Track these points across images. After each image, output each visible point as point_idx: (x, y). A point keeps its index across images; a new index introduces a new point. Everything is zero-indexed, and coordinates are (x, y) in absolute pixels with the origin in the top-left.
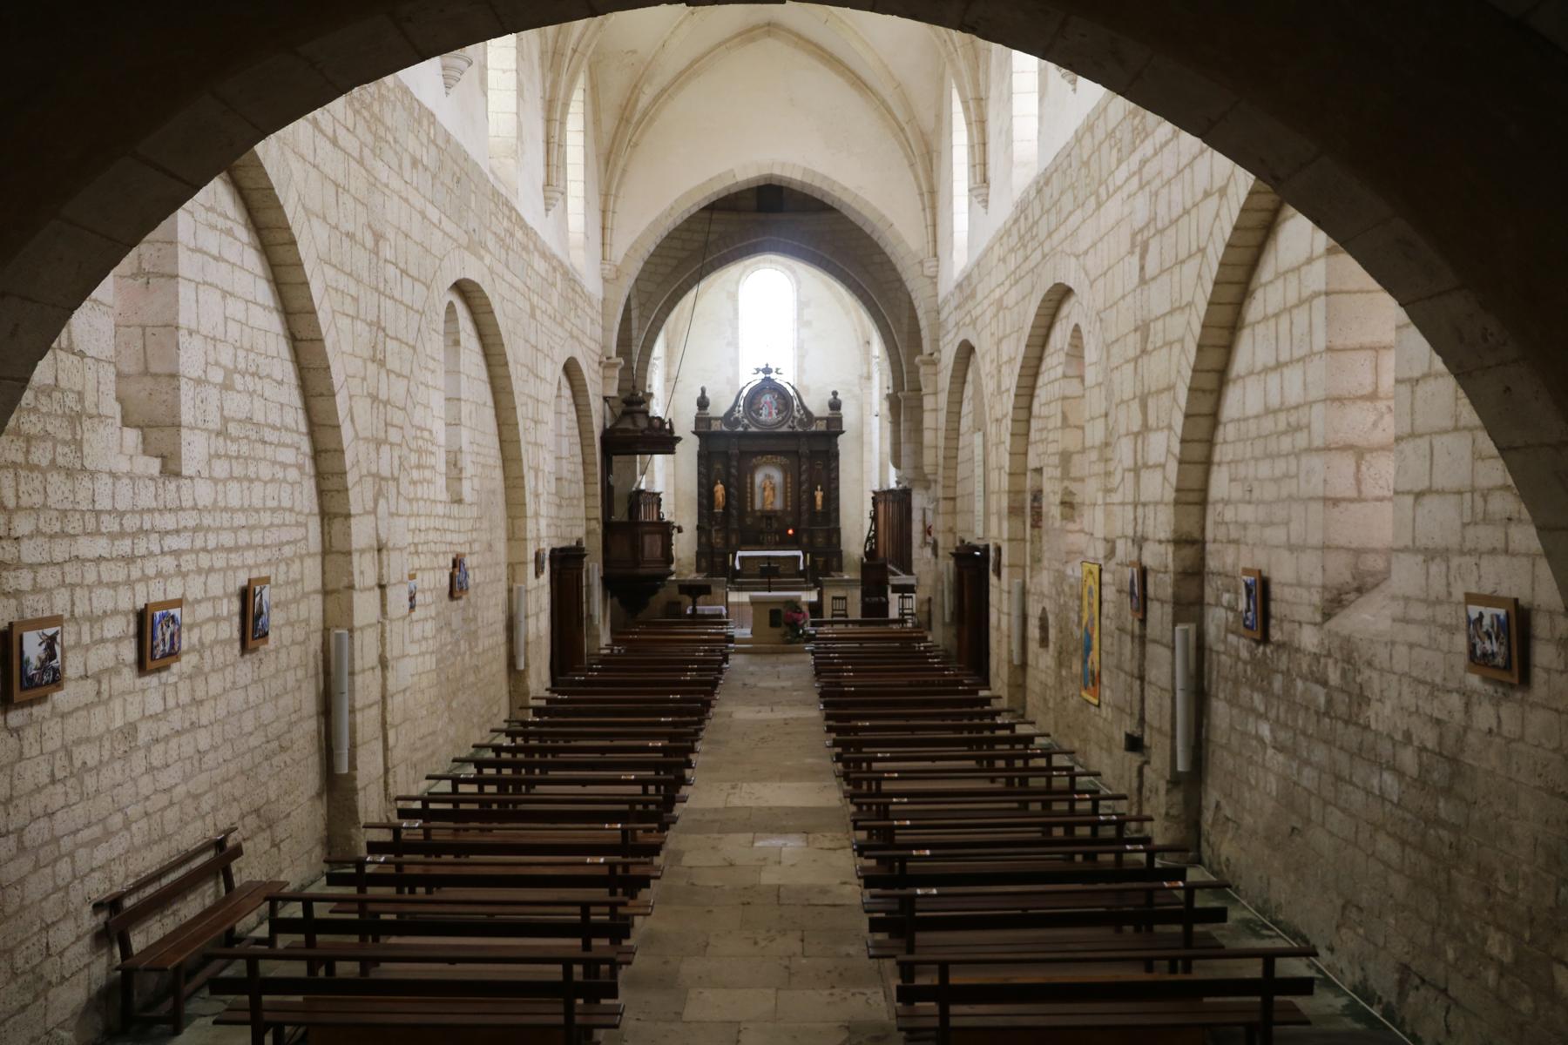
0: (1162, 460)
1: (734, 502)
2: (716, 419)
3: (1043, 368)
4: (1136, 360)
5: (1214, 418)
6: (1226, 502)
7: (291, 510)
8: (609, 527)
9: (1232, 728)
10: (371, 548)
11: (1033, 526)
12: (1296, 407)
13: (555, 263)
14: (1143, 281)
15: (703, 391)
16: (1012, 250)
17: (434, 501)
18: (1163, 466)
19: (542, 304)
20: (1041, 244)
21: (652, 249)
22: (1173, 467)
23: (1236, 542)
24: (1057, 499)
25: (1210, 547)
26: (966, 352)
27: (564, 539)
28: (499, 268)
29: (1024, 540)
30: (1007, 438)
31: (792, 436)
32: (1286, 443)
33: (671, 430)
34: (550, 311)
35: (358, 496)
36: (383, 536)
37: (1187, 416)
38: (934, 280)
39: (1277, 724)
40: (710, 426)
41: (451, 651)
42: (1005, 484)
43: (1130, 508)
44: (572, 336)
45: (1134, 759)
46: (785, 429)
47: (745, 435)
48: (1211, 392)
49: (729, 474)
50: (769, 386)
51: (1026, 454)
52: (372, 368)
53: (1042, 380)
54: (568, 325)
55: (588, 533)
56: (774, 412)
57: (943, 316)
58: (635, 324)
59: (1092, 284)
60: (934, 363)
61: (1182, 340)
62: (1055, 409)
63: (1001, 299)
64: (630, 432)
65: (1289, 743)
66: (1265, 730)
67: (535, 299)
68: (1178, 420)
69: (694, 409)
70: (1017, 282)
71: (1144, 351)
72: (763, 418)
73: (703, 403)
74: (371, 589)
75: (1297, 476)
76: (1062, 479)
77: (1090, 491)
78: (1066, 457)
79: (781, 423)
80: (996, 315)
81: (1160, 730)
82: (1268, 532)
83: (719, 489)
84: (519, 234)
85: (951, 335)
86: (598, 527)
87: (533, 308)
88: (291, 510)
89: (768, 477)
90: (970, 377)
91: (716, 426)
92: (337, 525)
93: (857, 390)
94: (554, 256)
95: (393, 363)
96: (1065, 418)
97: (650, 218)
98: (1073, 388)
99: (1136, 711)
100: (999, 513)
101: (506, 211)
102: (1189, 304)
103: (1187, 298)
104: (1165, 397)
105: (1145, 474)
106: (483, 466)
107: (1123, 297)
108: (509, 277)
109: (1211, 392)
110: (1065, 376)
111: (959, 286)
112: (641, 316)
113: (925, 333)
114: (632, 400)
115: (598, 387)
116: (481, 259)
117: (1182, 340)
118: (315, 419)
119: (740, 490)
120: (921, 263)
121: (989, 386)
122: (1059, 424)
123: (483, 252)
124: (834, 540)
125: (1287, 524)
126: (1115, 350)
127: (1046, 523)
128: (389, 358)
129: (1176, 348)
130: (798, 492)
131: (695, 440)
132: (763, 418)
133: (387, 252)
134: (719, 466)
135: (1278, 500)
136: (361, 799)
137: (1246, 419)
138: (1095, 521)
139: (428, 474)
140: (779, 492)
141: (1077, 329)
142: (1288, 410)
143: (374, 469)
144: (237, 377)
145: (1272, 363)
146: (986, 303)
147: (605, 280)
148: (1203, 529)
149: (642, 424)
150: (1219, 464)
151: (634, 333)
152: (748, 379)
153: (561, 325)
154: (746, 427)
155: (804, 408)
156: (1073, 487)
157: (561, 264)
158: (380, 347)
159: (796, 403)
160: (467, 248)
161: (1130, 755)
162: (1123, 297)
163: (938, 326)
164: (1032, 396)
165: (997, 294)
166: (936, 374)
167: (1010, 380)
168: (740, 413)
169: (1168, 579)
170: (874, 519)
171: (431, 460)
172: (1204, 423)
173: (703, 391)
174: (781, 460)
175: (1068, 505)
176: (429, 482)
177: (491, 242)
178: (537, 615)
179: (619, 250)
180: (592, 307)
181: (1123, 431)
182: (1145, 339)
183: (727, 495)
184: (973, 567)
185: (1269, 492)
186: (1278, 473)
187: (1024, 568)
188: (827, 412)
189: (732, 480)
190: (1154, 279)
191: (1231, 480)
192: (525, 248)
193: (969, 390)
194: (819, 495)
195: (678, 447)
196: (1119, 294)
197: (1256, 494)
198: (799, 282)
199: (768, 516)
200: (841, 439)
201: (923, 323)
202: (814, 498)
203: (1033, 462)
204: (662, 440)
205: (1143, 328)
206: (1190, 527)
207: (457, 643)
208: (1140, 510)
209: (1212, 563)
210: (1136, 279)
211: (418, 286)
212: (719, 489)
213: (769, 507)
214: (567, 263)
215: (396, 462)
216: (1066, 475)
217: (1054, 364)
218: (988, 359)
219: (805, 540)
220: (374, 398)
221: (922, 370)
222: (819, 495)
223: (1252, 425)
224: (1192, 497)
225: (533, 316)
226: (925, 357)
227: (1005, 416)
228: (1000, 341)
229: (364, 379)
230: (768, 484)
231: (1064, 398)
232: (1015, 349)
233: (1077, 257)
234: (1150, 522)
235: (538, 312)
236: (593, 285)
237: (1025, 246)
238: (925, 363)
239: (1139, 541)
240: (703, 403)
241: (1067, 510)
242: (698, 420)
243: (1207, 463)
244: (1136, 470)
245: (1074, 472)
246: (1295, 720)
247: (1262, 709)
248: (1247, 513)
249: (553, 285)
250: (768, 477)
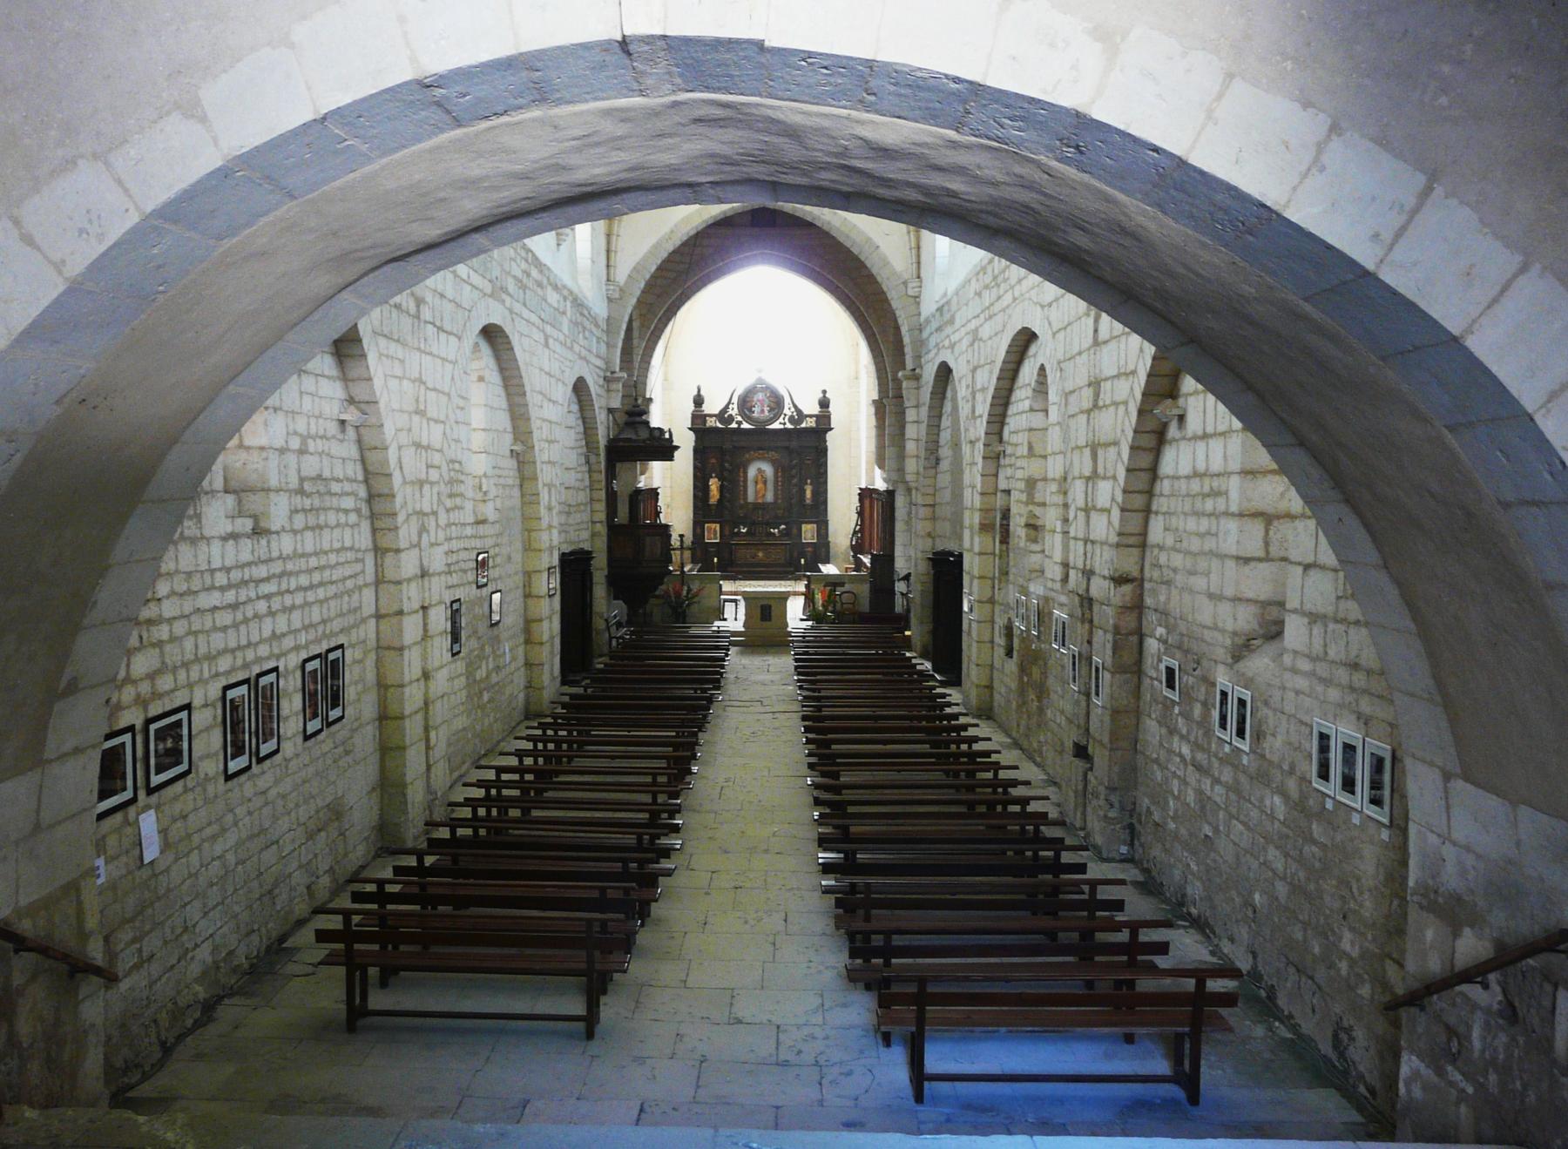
0: (1107, 505)
3: (1013, 399)
4: (1089, 412)
5: (1153, 472)
6: (1161, 548)
7: (351, 549)
8: (613, 530)
9: (1161, 744)
10: (416, 576)
11: (1001, 542)
12: (1218, 475)
13: (565, 292)
14: (1096, 343)
16: (986, 287)
17: (464, 524)
18: (1109, 511)
19: (555, 333)
20: (1012, 287)
21: (653, 268)
22: (1116, 513)
23: (1168, 583)
24: (1023, 521)
25: (1147, 585)
26: (945, 372)
27: (571, 543)
28: (518, 307)
29: (994, 554)
30: (980, 460)
32: (1209, 505)
33: (671, 439)
34: (562, 338)
35: (406, 533)
36: (425, 563)
37: (1128, 470)
38: (916, 299)
39: (1196, 746)
41: (478, 656)
42: (977, 504)
43: (1081, 543)
44: (581, 358)
45: (1080, 764)
46: (776, 426)
47: (739, 431)
48: (1150, 450)
49: (722, 466)
51: (996, 475)
52: (416, 419)
53: (1012, 410)
54: (577, 348)
55: (593, 535)
57: (925, 335)
58: (636, 334)
59: (1054, 334)
60: (917, 378)
61: (1126, 403)
62: (1022, 438)
63: (976, 330)
64: (635, 441)
65: (1205, 763)
66: (1186, 750)
67: (548, 329)
68: (1121, 474)
69: (692, 407)
70: (990, 317)
71: (1095, 406)
73: (698, 401)
74: (416, 612)
75: (1216, 535)
76: (1027, 504)
77: (1051, 518)
78: (1031, 483)
80: (972, 345)
81: (1100, 742)
82: (1192, 579)
83: (714, 484)
84: (535, 273)
85: (931, 355)
86: (602, 529)
87: (547, 338)
88: (351, 549)
89: (759, 470)
90: (949, 394)
92: (389, 559)
94: (565, 287)
95: (432, 412)
96: (1030, 448)
97: (653, 240)
98: (1037, 420)
99: (1082, 722)
100: (971, 528)
101: (523, 254)
102: (1134, 372)
103: (1131, 367)
104: (1112, 450)
105: (1093, 515)
106: (504, 486)
107: (1080, 353)
108: (526, 314)
109: (1150, 450)
110: (1032, 410)
111: (940, 310)
112: (642, 325)
113: (908, 350)
114: (635, 411)
115: (605, 401)
116: (503, 302)
117: (1126, 403)
118: (370, 468)
120: (905, 283)
121: (964, 410)
122: (1025, 452)
123: (504, 296)
125: (1208, 574)
126: (1072, 399)
127: (1013, 541)
128: (429, 409)
129: (1122, 408)
131: (691, 436)
133: (426, 314)
135: (1202, 553)
136: (409, 791)
137: (1178, 478)
138: (1054, 544)
139: (458, 501)
140: (770, 486)
141: (1042, 368)
142: (1212, 476)
143: (418, 508)
144: (310, 441)
145: (1200, 433)
146: (963, 331)
147: (610, 300)
148: (1142, 570)
149: (644, 434)
150: (1157, 513)
151: (635, 342)
153: (571, 348)
154: (739, 423)
156: (1038, 511)
157: (571, 293)
158: (422, 399)
159: (787, 401)
160: (491, 296)
161: (1077, 761)
162: (1080, 353)
163: (920, 344)
164: (1002, 424)
165: (972, 325)
166: (918, 388)
167: (983, 407)
168: (734, 411)
169: (1109, 611)
171: (462, 488)
172: (1145, 476)
175: (1034, 527)
176: (460, 508)
177: (511, 287)
178: (550, 618)
179: (621, 275)
180: (597, 325)
181: (1077, 474)
182: (1097, 395)
183: (722, 489)
184: (946, 571)
185: (1195, 544)
186: (1202, 529)
187: (993, 579)
188: (816, 410)
190: (1105, 342)
191: (1166, 529)
192: (540, 285)
193: (948, 407)
195: (676, 454)
196: (1076, 350)
197: (1185, 544)
199: (759, 507)
200: (829, 435)
201: (906, 340)
203: (1002, 485)
204: (663, 448)
205: (1095, 384)
206: (1129, 565)
207: (482, 648)
208: (1089, 546)
209: (1148, 601)
210: (1090, 340)
211: (452, 338)
212: (714, 484)
214: (575, 290)
215: (435, 497)
216: (1031, 500)
217: (1022, 397)
218: (964, 383)
220: (418, 445)
221: (904, 384)
223: (1183, 484)
224: (1131, 540)
225: (547, 345)
226: (907, 373)
227: (978, 440)
228: (974, 370)
229: (410, 430)
231: (1031, 430)
232: (988, 379)
233: (1042, 307)
234: (1097, 558)
235: (551, 341)
236: (600, 309)
237: (998, 286)
238: (907, 378)
239: (1088, 574)
240: (698, 401)
241: (1032, 532)
243: (1147, 511)
244: (1087, 510)
245: (1038, 498)
246: (1209, 743)
247: (1184, 732)
248: (1177, 560)
249: (564, 313)
250: (759, 470)
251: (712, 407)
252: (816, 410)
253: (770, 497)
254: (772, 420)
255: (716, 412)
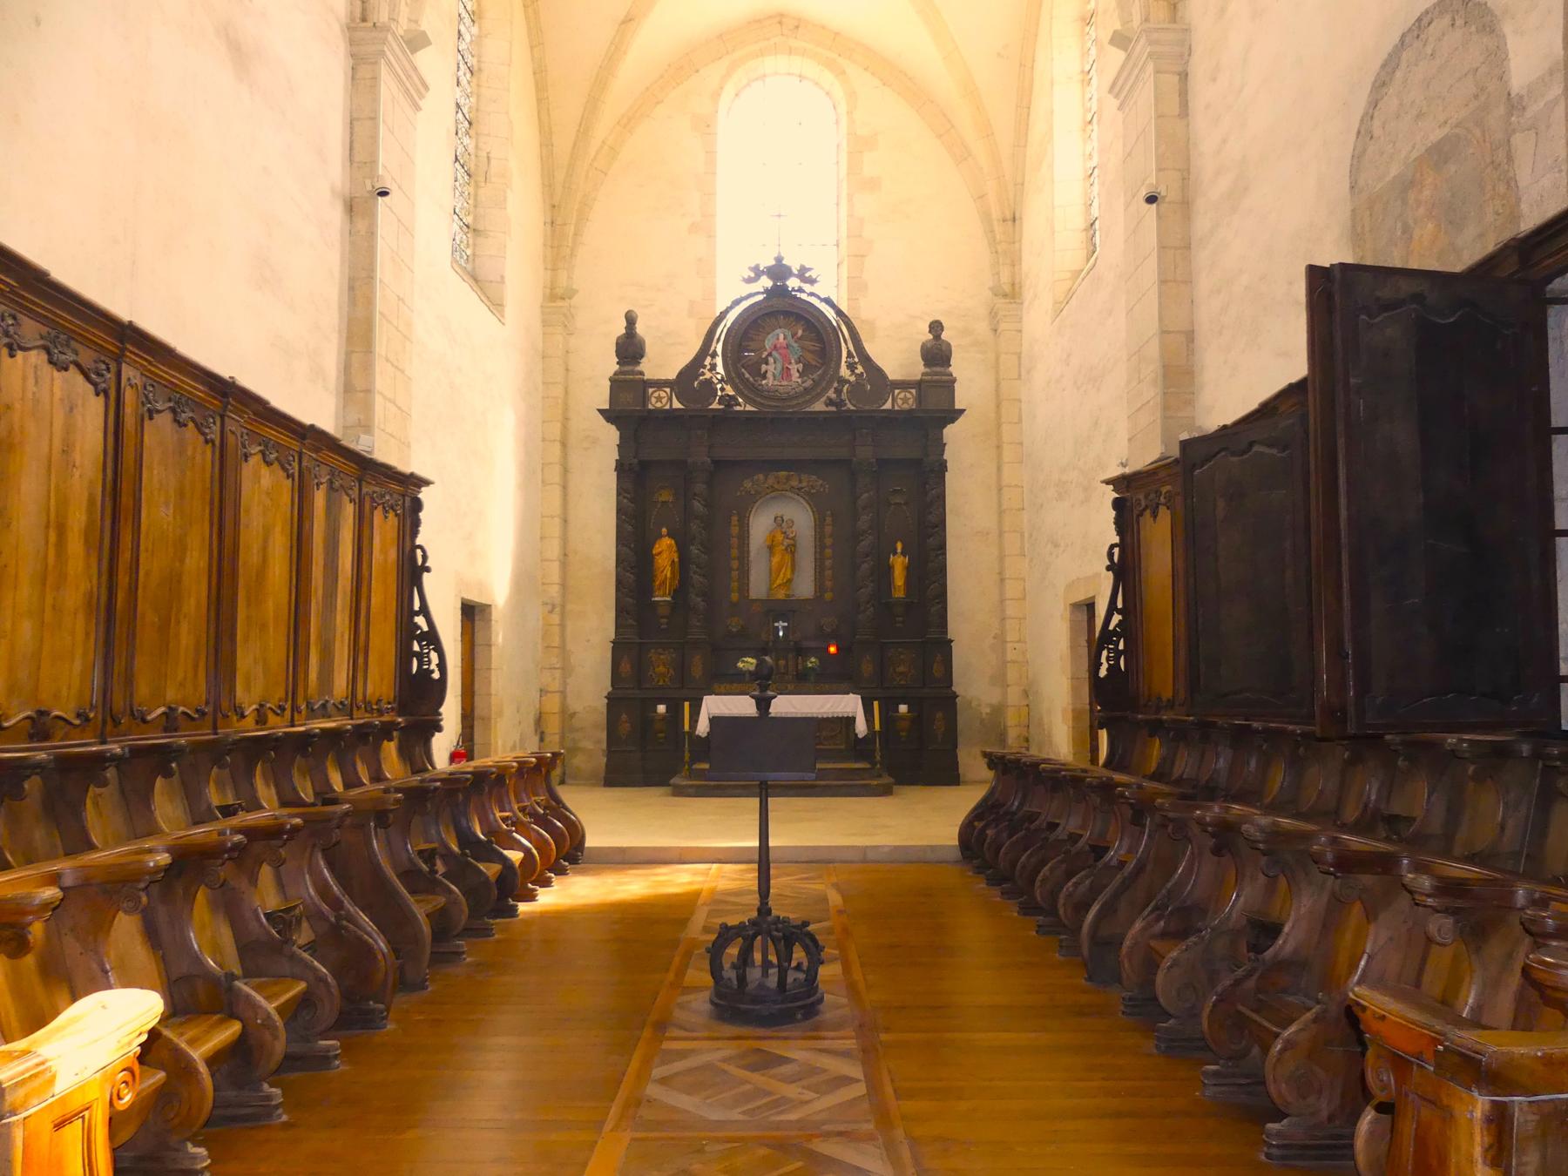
1: (697, 579)
2: (660, 384)
15: (631, 320)
31: (839, 421)
40: (645, 398)
46: (819, 406)
47: (727, 419)
50: (782, 312)
56: (795, 368)
69: (612, 365)
72: (769, 382)
73: (630, 349)
79: (812, 393)
83: (665, 551)
89: (779, 520)
91: (661, 400)
93: (982, 328)
119: (713, 549)
124: (937, 670)
130: (849, 551)
131: (610, 435)
132: (769, 382)
134: (666, 496)
152: (733, 291)
154: (729, 401)
155: (866, 360)
170: (1125, 567)
173: (631, 320)
174: (807, 480)
183: (684, 563)
188: (917, 369)
189: (694, 527)
194: (899, 563)
198: (852, 96)
200: (950, 432)
202: (890, 569)
212: (665, 551)
213: (781, 595)
219: (867, 668)
222: (899, 563)
230: (780, 541)
240: (630, 349)
242: (617, 384)
251: (664, 361)
252: (917, 369)
253: (805, 588)
254: (812, 393)
255: (672, 375)
